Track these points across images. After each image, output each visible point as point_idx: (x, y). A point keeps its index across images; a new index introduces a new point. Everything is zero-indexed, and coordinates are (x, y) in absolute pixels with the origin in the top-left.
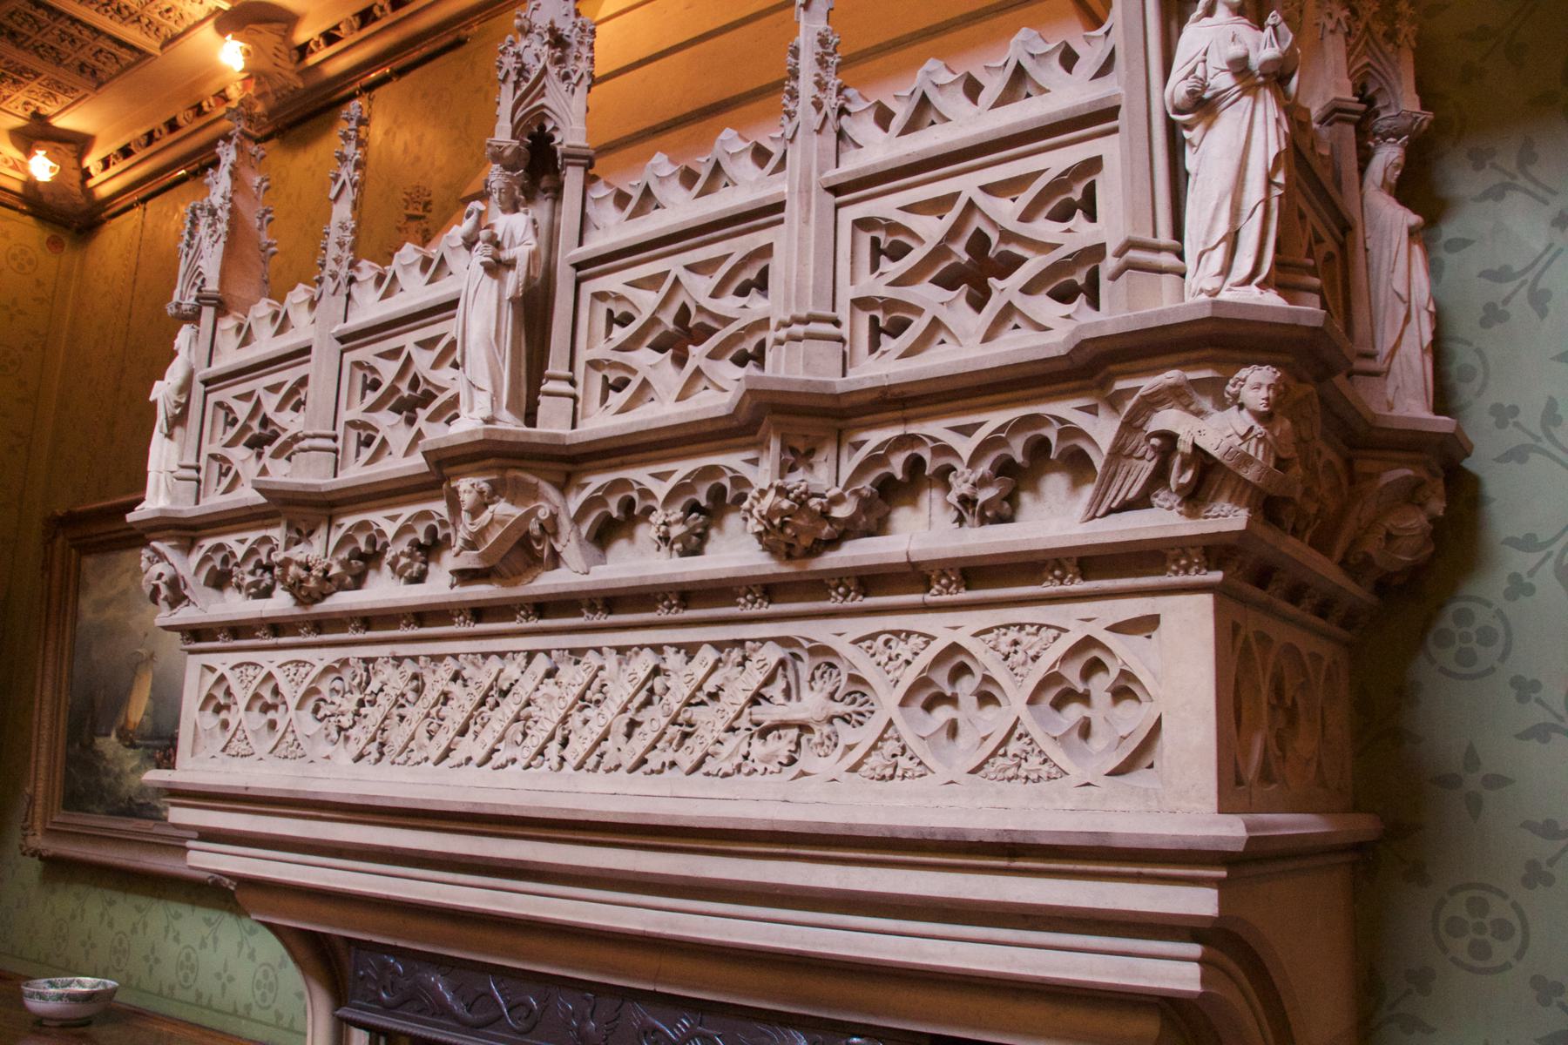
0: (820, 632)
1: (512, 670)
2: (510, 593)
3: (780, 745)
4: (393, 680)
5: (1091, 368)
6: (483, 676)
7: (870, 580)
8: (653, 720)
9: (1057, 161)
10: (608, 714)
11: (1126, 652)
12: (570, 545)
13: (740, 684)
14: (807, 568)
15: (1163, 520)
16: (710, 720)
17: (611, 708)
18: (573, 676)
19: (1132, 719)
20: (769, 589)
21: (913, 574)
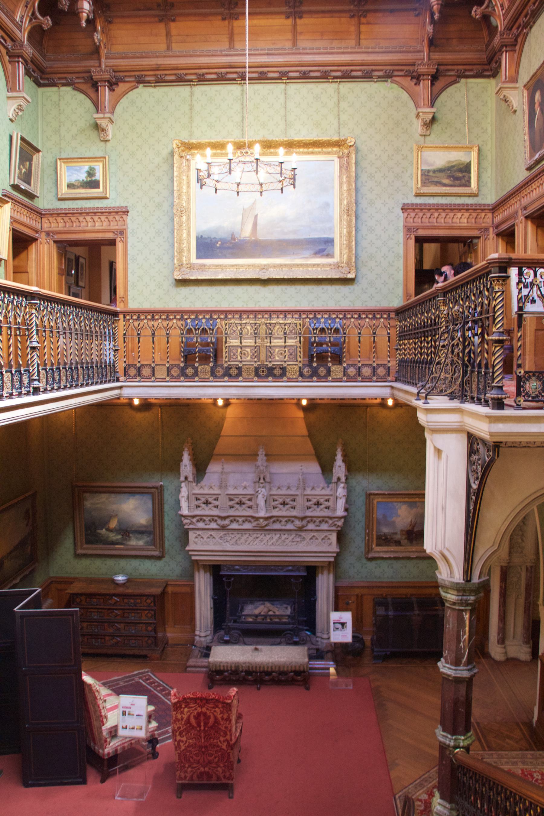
0: (300, 533)
1: (259, 535)
2: (262, 529)
3: (295, 543)
4: (239, 536)
5: (331, 518)
6: (255, 536)
7: (306, 530)
8: (280, 541)
9: (327, 497)
10: (274, 540)
11: (330, 537)
12: (271, 524)
13: (290, 538)
14: (301, 529)
15: (334, 528)
16: (287, 541)
17: (274, 540)
18: (268, 537)
19: (329, 541)
20: (295, 530)
21: (312, 530)
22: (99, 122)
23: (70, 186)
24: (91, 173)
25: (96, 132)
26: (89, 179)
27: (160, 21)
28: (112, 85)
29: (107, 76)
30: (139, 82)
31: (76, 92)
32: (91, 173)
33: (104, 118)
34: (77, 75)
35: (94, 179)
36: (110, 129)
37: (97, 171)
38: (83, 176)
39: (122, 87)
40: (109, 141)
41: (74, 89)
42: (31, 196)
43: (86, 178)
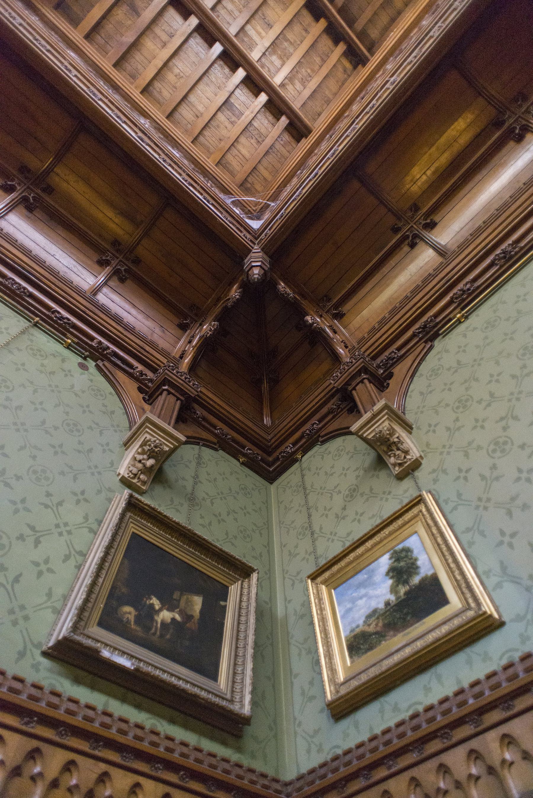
22: (369, 434)
23: (358, 644)
24: (403, 568)
25: (383, 474)
26: (403, 590)
27: (413, 246)
28: (381, 383)
29: (359, 365)
30: (433, 338)
31: (327, 445)
32: (403, 568)
33: (374, 416)
34: (318, 416)
35: (416, 580)
36: (412, 445)
37: (416, 553)
38: (377, 590)
39: (399, 370)
40: (416, 465)
41: (323, 442)
42: (227, 724)
43: (393, 590)
